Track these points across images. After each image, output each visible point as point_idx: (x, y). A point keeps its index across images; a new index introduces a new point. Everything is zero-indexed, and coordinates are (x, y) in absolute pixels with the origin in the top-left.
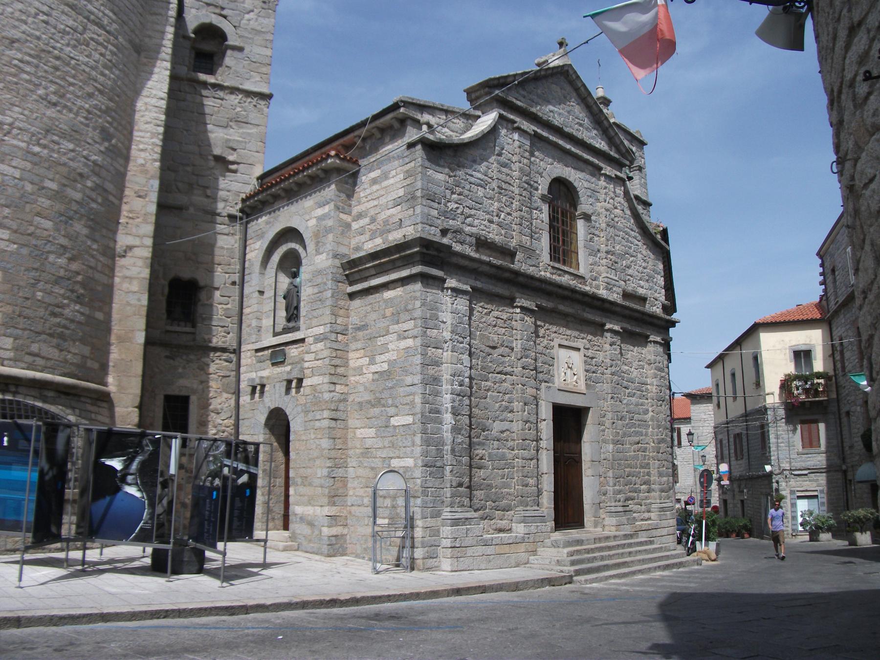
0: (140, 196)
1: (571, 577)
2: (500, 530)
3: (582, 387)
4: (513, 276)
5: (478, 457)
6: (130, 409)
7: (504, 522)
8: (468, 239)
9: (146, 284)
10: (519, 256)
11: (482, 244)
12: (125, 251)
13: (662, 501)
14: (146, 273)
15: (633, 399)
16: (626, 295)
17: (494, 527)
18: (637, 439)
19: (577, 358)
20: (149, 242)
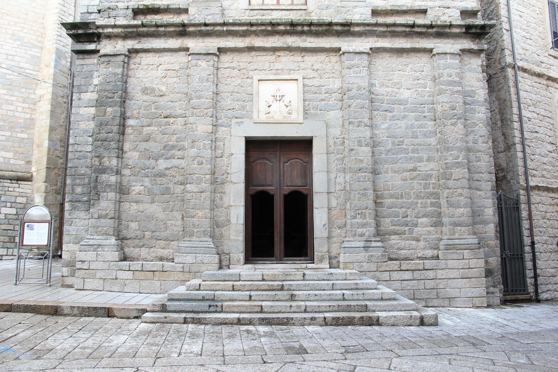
0: (47, 66)
1: (145, 311)
2: (161, 259)
3: (297, 116)
4: (181, 28)
5: (134, 193)
6: (41, 184)
7: (166, 251)
8: (122, 12)
9: (49, 113)
10: (191, 11)
11: (137, 12)
12: (40, 97)
13: (456, 236)
14: (49, 107)
15: (402, 124)
16: (375, 13)
17: (154, 255)
18: (411, 166)
19: (292, 92)
20: (50, 90)
